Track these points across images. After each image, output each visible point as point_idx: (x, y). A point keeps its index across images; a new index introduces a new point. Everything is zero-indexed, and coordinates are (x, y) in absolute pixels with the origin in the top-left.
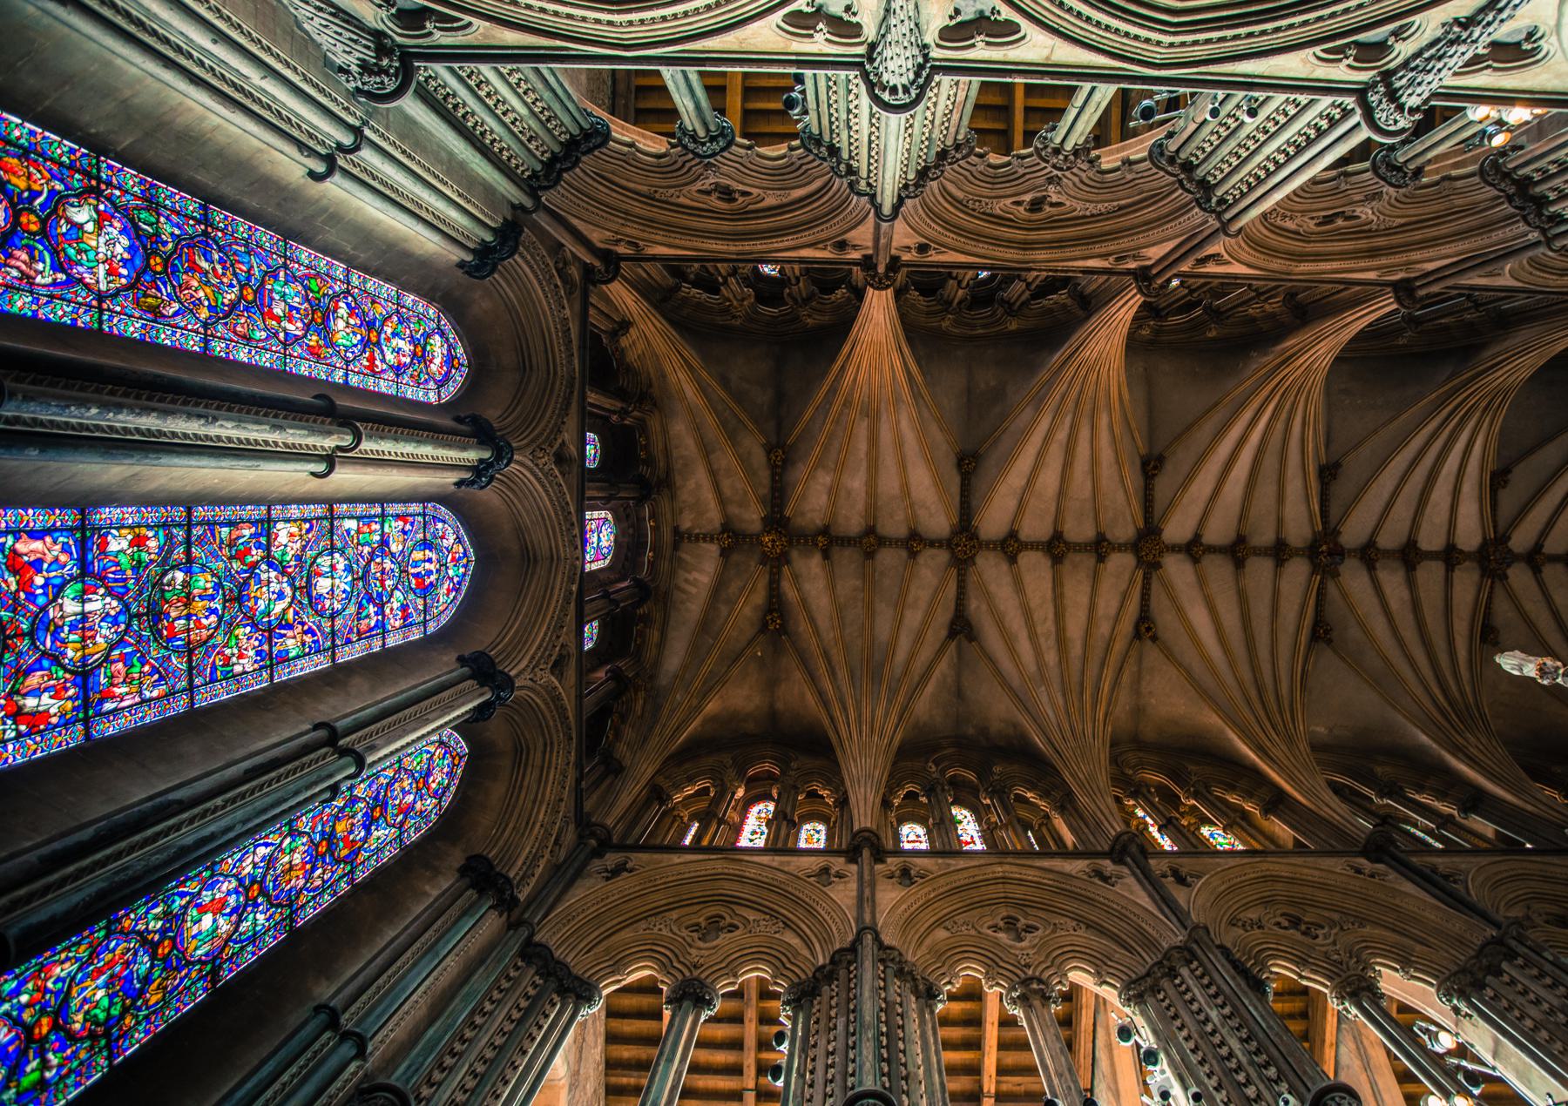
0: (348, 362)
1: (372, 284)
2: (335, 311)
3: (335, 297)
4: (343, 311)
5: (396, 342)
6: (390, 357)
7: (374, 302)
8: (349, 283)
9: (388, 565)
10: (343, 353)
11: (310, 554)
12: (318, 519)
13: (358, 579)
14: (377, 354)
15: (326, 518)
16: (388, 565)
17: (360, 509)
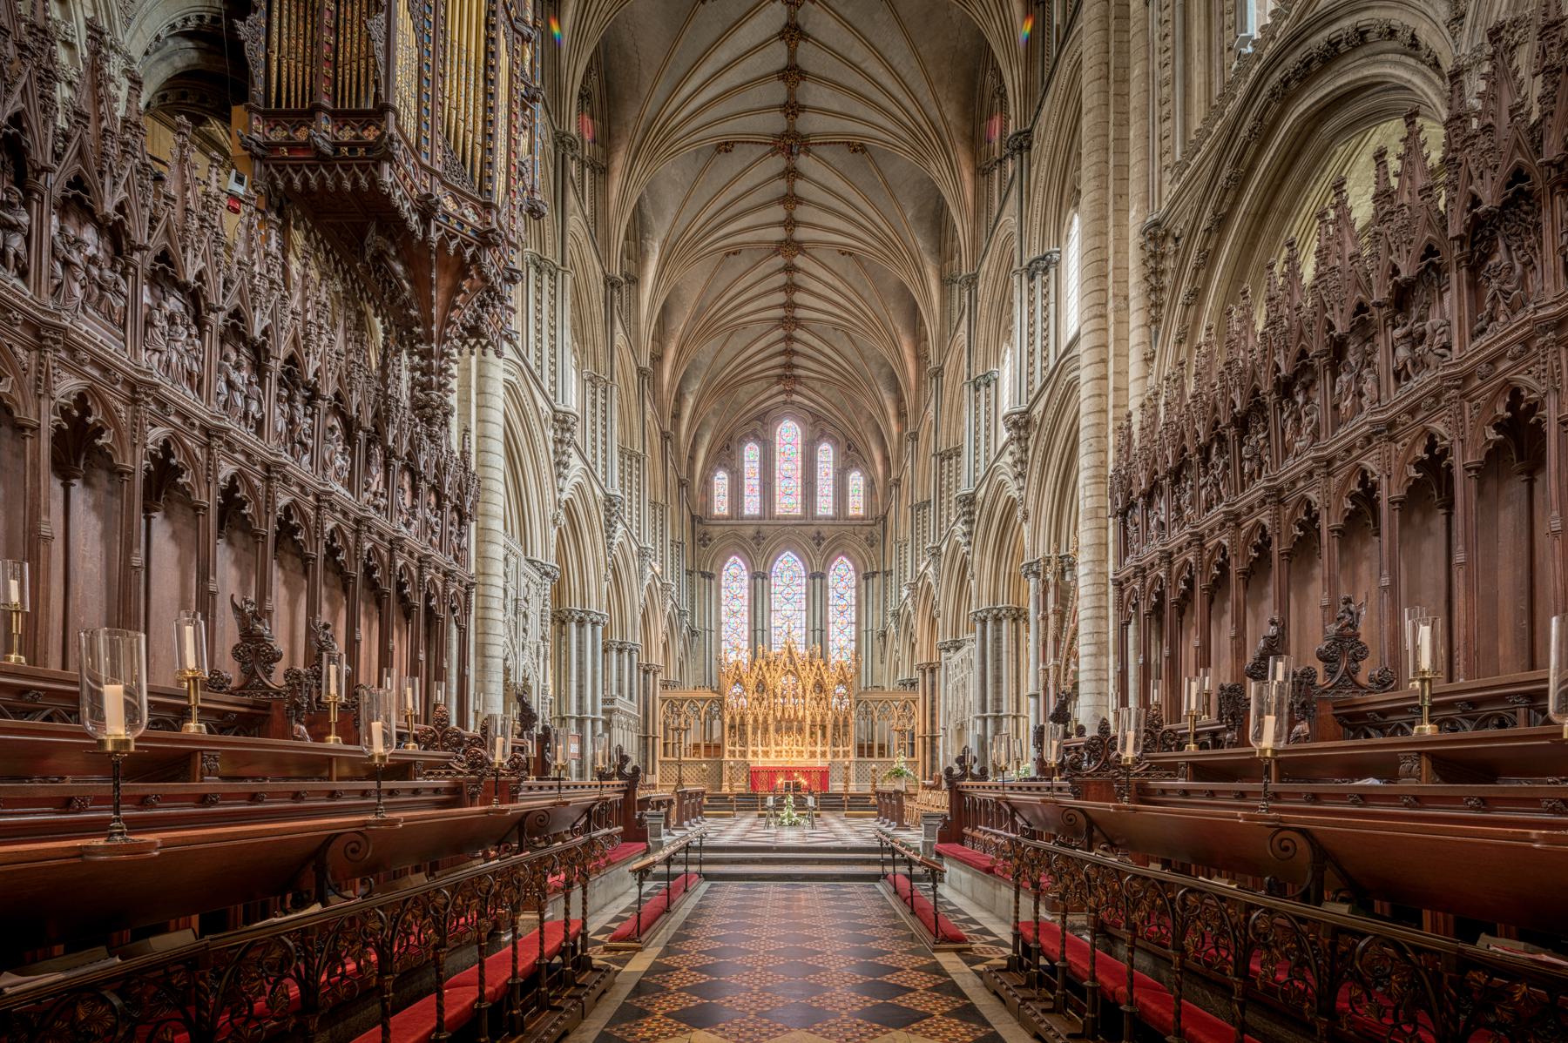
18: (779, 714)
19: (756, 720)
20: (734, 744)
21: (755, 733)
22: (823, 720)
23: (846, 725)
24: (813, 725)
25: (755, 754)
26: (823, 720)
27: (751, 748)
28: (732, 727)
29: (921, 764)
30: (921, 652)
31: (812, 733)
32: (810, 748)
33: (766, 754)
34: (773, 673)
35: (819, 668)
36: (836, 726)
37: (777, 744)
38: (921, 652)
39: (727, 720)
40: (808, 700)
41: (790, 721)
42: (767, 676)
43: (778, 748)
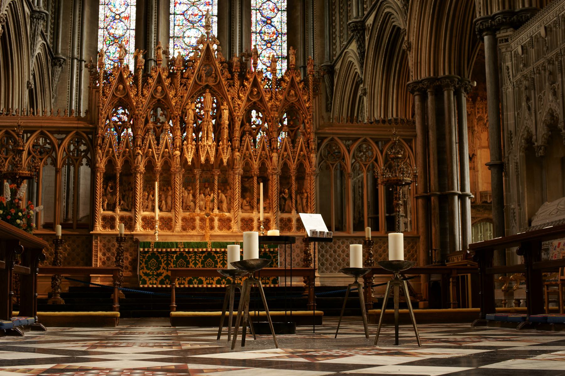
0: (127, 29)
1: (101, 17)
2: (113, 34)
3: (109, 33)
4: (112, 31)
5: (118, 7)
6: (123, 9)
7: (107, 17)
8: (103, 28)
9: (190, 12)
10: (125, 31)
11: (184, 46)
12: (174, 43)
13: (193, 26)
14: (122, 15)
15: (174, 39)
16: (190, 12)
17: (172, 24)
18: (189, 157)
19: (150, 166)
20: (111, 207)
21: (149, 187)
22: (263, 167)
23: (301, 178)
24: (246, 177)
25: (148, 223)
26: (263, 167)
27: (141, 214)
28: (109, 177)
29: (422, 238)
30: (418, 64)
31: (246, 191)
32: (242, 214)
33: (167, 224)
34: (180, 89)
35: (255, 84)
36: (284, 179)
37: (186, 208)
38: (418, 64)
39: (102, 165)
40: (237, 134)
41: (207, 167)
42: (171, 94)
43: (187, 214)
